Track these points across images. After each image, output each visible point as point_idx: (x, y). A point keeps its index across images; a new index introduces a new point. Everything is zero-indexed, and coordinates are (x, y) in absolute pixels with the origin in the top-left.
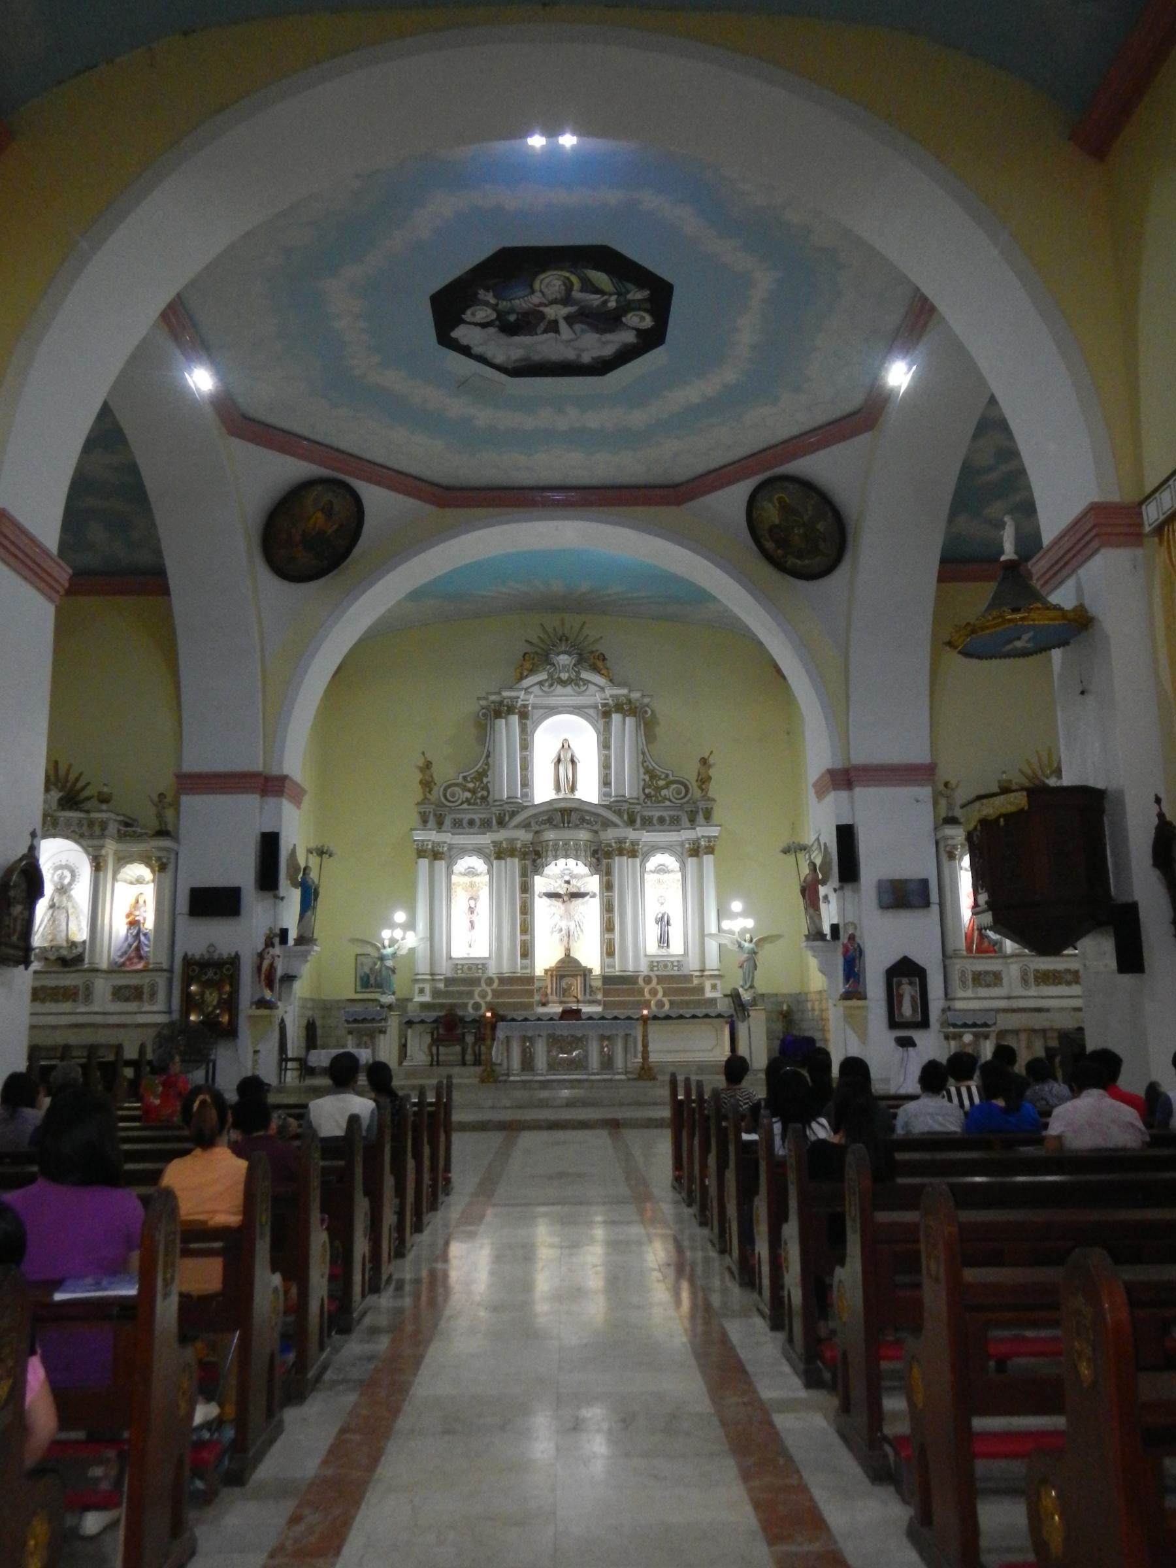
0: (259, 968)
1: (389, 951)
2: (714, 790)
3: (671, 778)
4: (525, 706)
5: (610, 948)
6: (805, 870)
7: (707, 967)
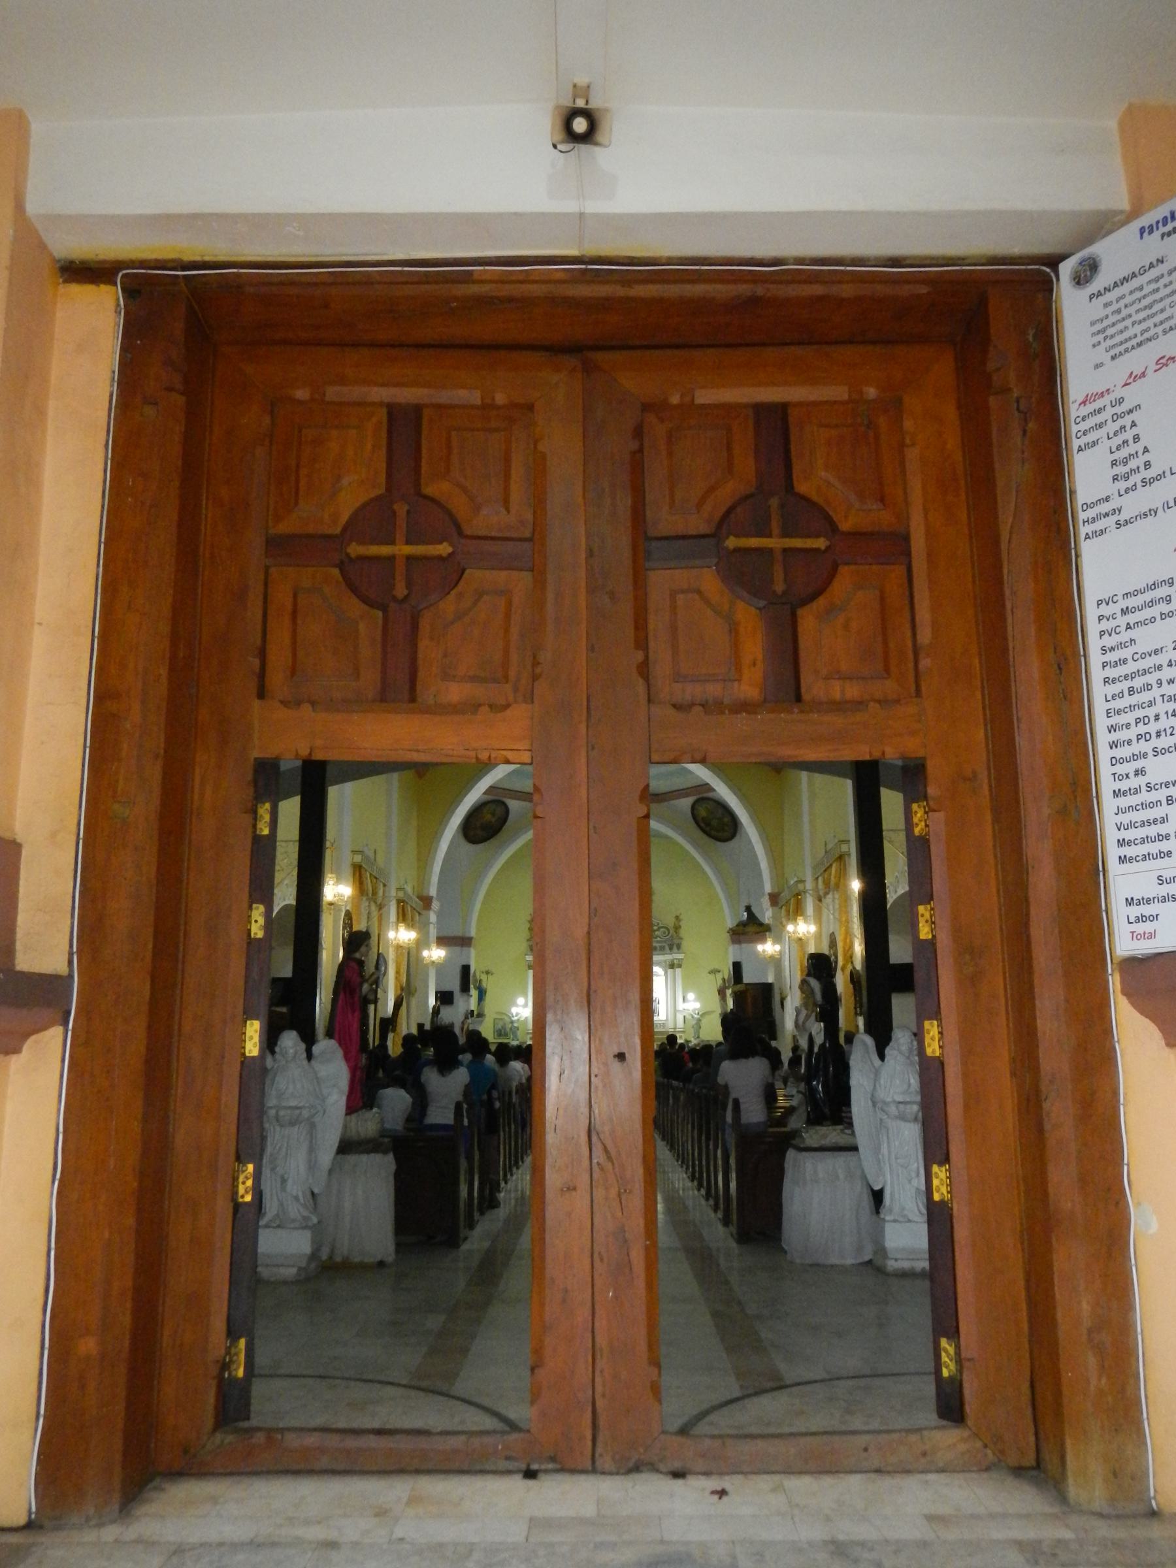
0: (462, 1029)
1: (515, 1018)
2: (682, 933)
3: (660, 925)
6: (720, 982)
7: (678, 1026)
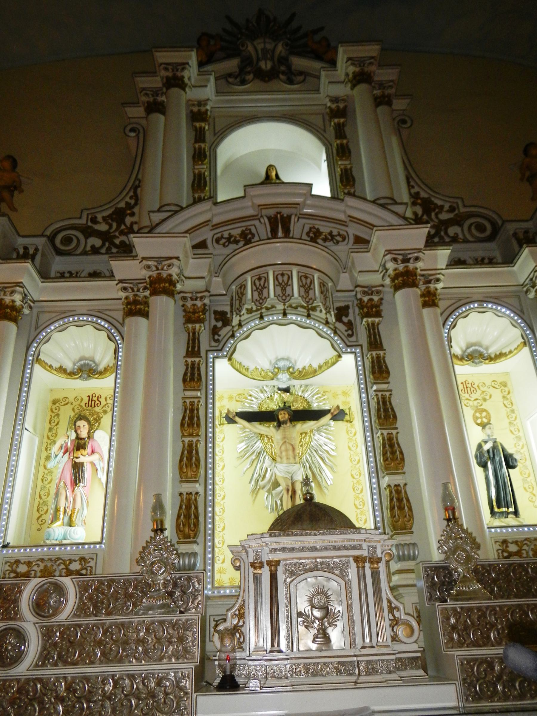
3: (462, 210)
4: (201, 103)
5: (401, 508)
